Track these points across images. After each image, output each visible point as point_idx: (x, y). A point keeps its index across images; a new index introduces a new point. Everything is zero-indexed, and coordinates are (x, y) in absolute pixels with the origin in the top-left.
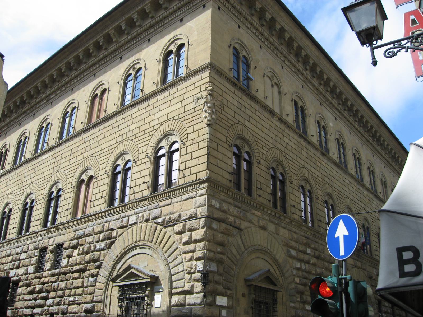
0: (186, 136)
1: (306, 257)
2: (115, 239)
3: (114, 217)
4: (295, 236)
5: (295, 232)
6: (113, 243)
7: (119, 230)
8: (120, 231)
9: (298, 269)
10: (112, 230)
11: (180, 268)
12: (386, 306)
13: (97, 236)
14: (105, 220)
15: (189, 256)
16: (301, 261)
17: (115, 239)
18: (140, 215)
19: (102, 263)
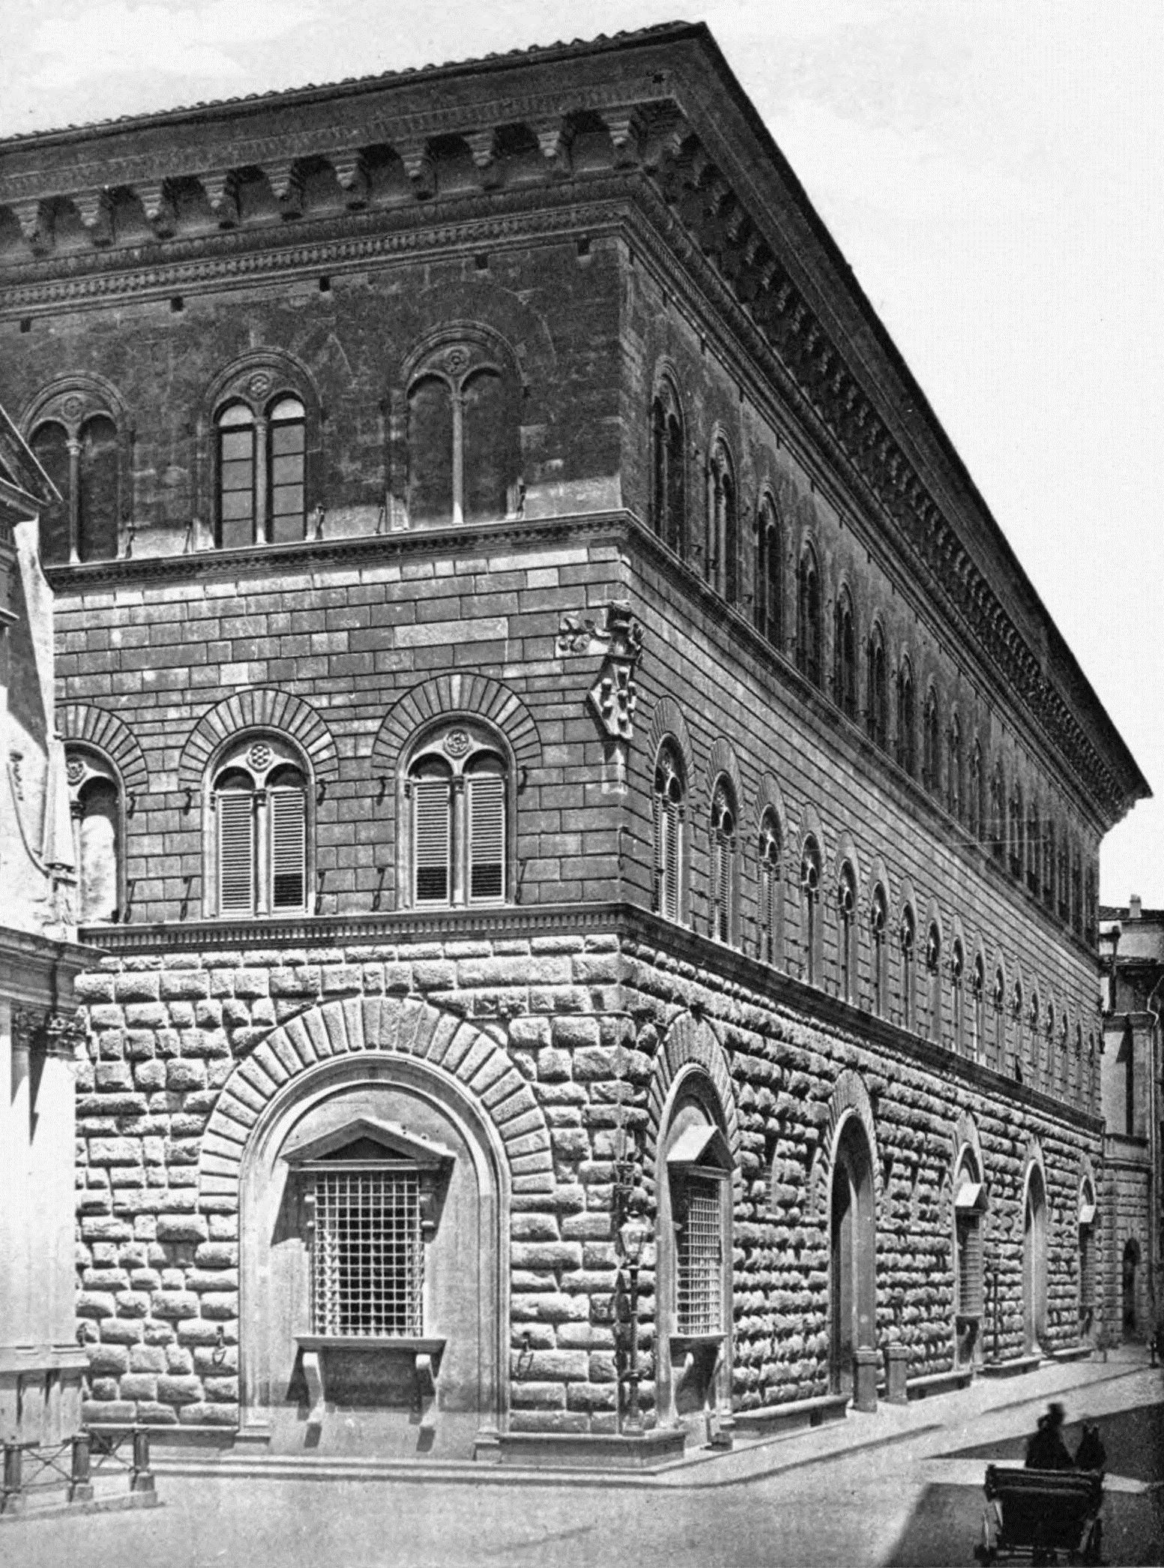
0: (536, 749)
1: (764, 1066)
2: (264, 1029)
3: (255, 956)
4: (745, 1007)
5: (744, 999)
6: (256, 1040)
7: (282, 1003)
8: (286, 1007)
9: (749, 1108)
10: (249, 998)
11: (531, 1141)
12: (900, 1177)
13: (183, 1009)
14: (212, 957)
15: (574, 1113)
16: (758, 1082)
17: (264, 1029)
18: (370, 967)
19: (217, 1096)
